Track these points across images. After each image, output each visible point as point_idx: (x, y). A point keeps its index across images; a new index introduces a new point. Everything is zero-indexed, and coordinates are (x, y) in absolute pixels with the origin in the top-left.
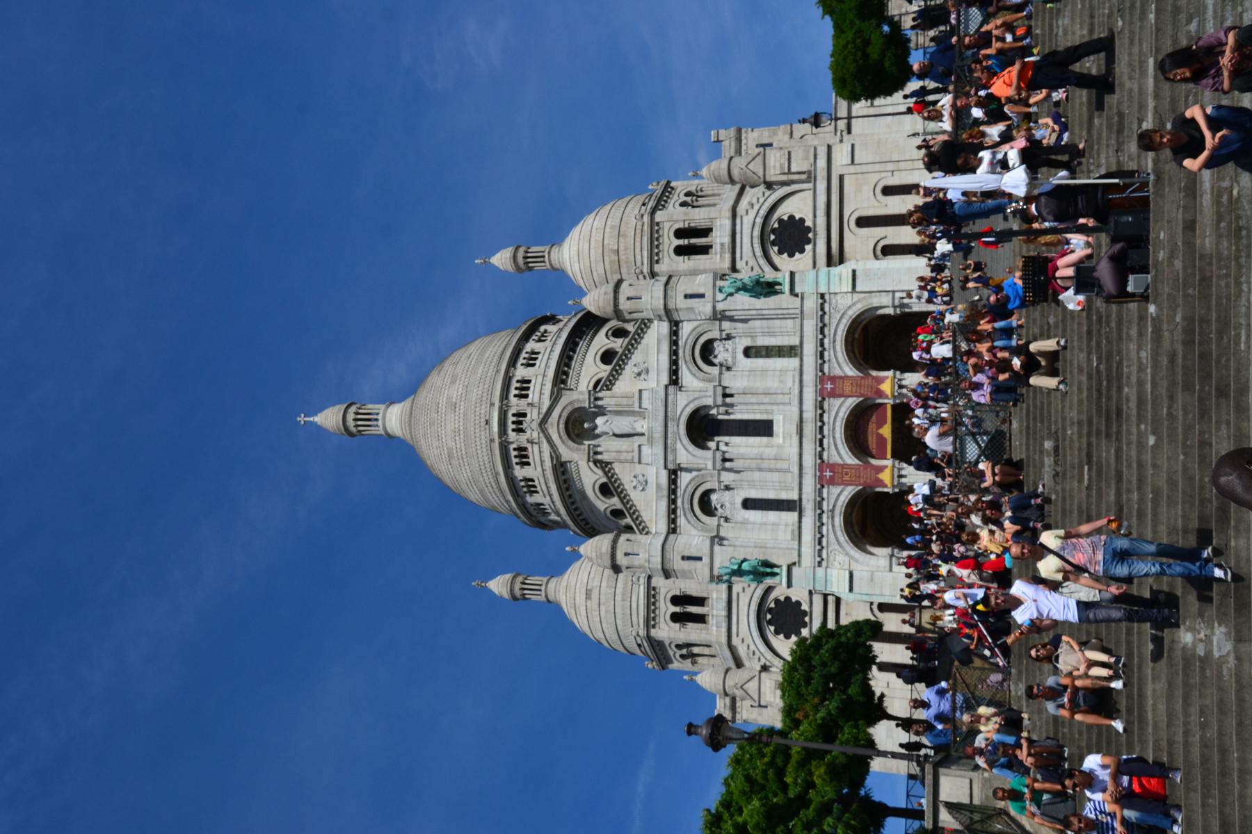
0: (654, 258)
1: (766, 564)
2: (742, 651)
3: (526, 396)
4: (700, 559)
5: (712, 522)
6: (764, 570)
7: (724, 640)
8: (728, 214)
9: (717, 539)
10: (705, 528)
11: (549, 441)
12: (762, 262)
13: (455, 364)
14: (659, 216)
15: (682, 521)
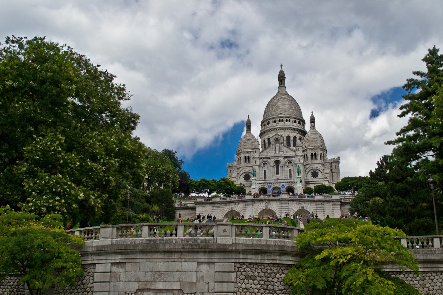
0: (310, 149)
1: (255, 176)
2: (241, 169)
3: (286, 122)
4: (256, 163)
5: (262, 165)
6: (254, 175)
7: (242, 166)
8: (319, 163)
9: (259, 166)
10: (261, 164)
11: (274, 136)
12: (310, 169)
13: (293, 104)
14: (319, 150)
15: (262, 160)
